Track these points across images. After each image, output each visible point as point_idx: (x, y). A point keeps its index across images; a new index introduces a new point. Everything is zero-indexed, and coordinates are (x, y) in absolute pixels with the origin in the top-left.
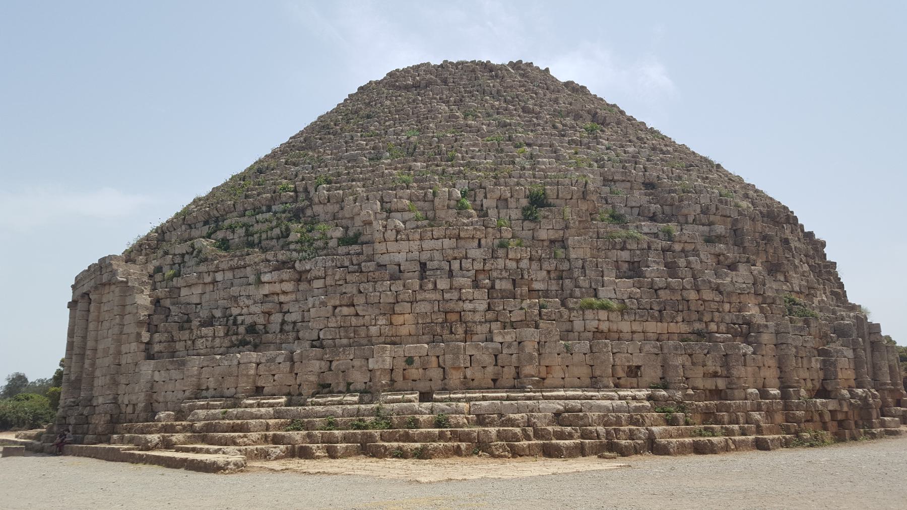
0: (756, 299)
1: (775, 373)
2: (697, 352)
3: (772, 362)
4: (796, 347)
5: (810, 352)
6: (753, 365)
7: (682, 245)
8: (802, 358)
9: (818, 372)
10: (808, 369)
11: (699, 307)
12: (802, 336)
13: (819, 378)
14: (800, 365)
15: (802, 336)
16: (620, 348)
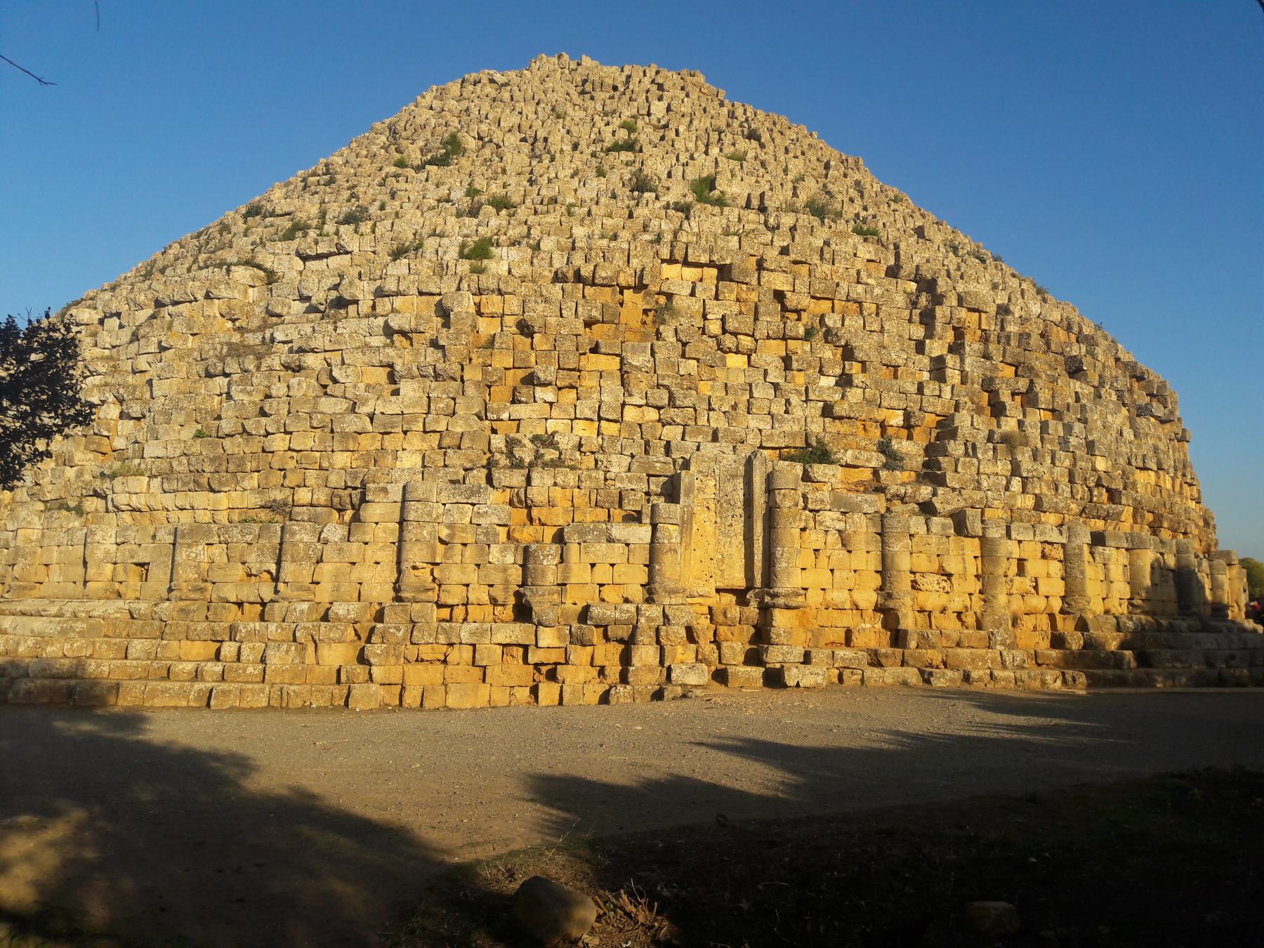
0: (424, 440)
1: (387, 573)
2: (235, 540)
3: (388, 556)
4: (451, 526)
5: (487, 534)
6: (337, 560)
7: (321, 356)
8: (465, 545)
9: (505, 570)
10: (478, 565)
11: (286, 463)
12: (473, 505)
13: (506, 583)
14: (458, 559)
15: (473, 505)
16: (124, 537)
